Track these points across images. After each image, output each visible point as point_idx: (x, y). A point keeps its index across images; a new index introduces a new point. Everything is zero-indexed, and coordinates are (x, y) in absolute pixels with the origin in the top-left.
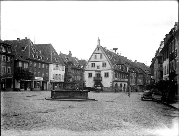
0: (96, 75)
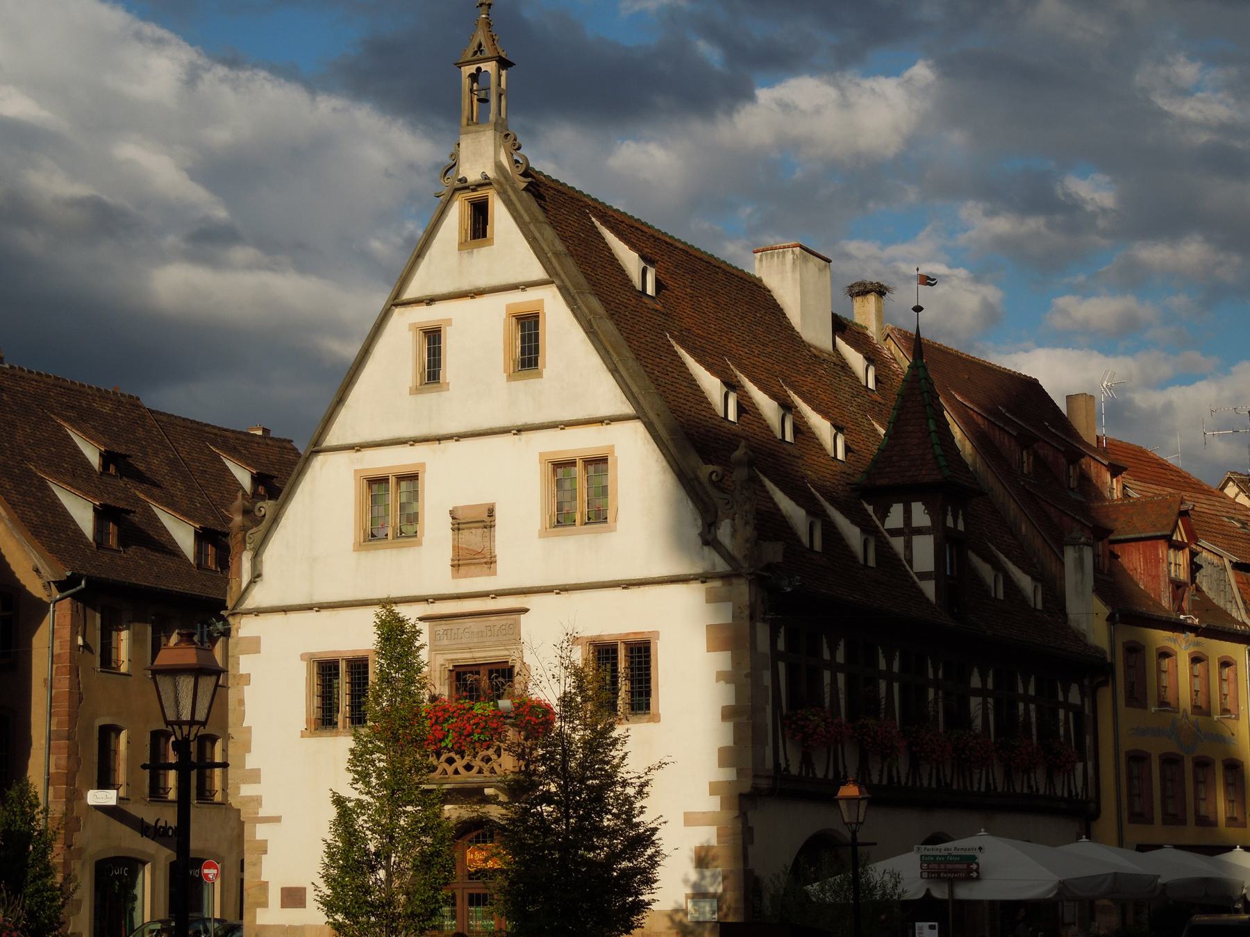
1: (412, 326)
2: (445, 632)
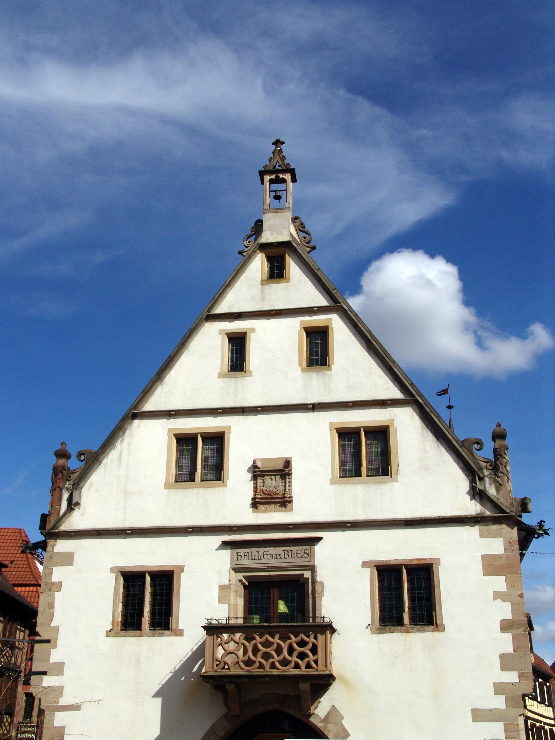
1: (220, 332)
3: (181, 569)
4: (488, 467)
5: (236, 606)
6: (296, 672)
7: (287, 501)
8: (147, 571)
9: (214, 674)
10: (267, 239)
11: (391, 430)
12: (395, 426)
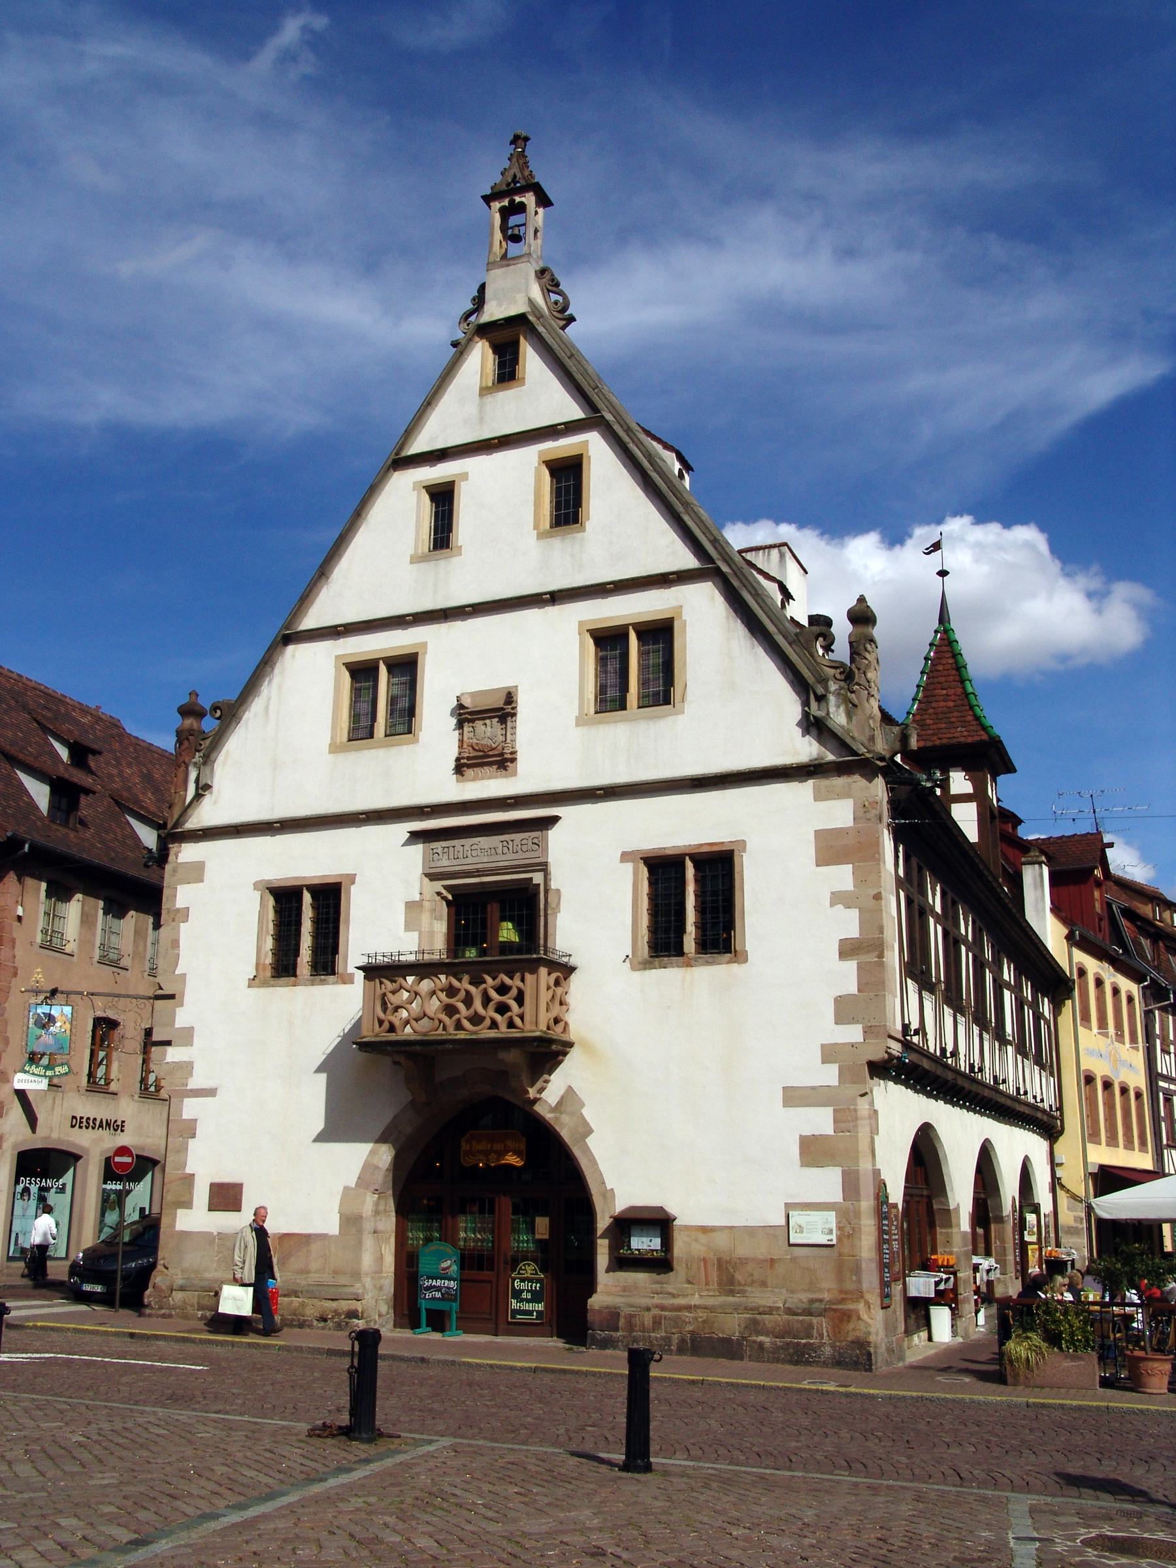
0: (439, 929)
2: (446, 850)
3: (352, 879)
4: (838, 676)
5: (431, 934)
6: (492, 1034)
7: (507, 760)
8: (304, 886)
9: (373, 1039)
10: (491, 315)
11: (677, 625)
12: (684, 618)
